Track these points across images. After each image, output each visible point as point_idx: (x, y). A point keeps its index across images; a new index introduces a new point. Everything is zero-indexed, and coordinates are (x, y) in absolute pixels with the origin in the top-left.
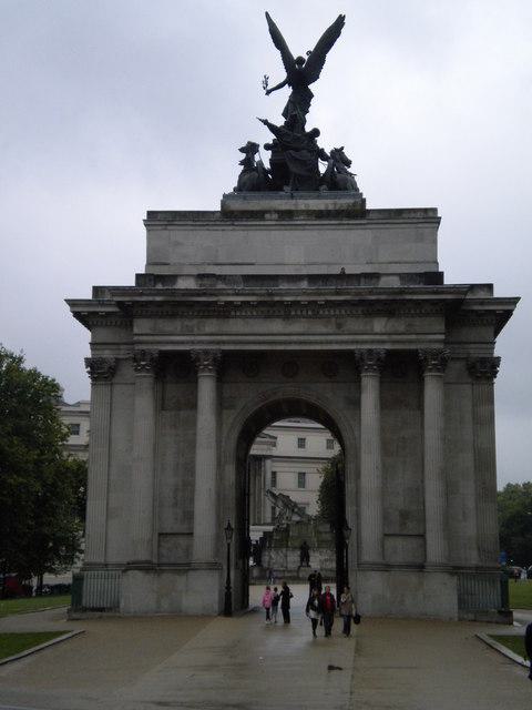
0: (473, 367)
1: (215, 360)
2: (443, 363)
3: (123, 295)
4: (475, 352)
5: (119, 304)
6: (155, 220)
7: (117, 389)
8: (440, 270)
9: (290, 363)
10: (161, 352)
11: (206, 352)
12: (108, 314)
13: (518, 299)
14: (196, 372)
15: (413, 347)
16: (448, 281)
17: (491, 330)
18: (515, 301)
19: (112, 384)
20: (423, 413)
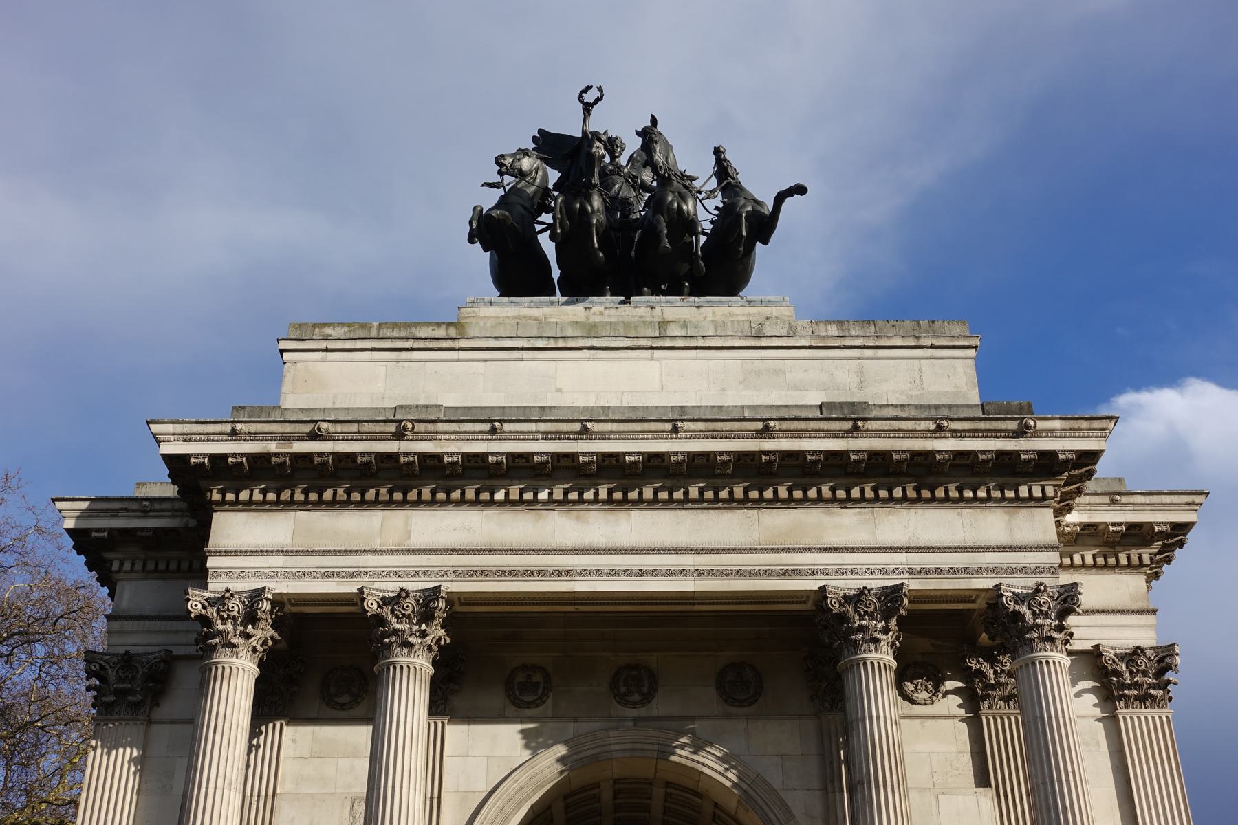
0: (1116, 673)
3: (187, 438)
5: (176, 464)
10: (279, 602)
11: (403, 593)
19: (150, 722)
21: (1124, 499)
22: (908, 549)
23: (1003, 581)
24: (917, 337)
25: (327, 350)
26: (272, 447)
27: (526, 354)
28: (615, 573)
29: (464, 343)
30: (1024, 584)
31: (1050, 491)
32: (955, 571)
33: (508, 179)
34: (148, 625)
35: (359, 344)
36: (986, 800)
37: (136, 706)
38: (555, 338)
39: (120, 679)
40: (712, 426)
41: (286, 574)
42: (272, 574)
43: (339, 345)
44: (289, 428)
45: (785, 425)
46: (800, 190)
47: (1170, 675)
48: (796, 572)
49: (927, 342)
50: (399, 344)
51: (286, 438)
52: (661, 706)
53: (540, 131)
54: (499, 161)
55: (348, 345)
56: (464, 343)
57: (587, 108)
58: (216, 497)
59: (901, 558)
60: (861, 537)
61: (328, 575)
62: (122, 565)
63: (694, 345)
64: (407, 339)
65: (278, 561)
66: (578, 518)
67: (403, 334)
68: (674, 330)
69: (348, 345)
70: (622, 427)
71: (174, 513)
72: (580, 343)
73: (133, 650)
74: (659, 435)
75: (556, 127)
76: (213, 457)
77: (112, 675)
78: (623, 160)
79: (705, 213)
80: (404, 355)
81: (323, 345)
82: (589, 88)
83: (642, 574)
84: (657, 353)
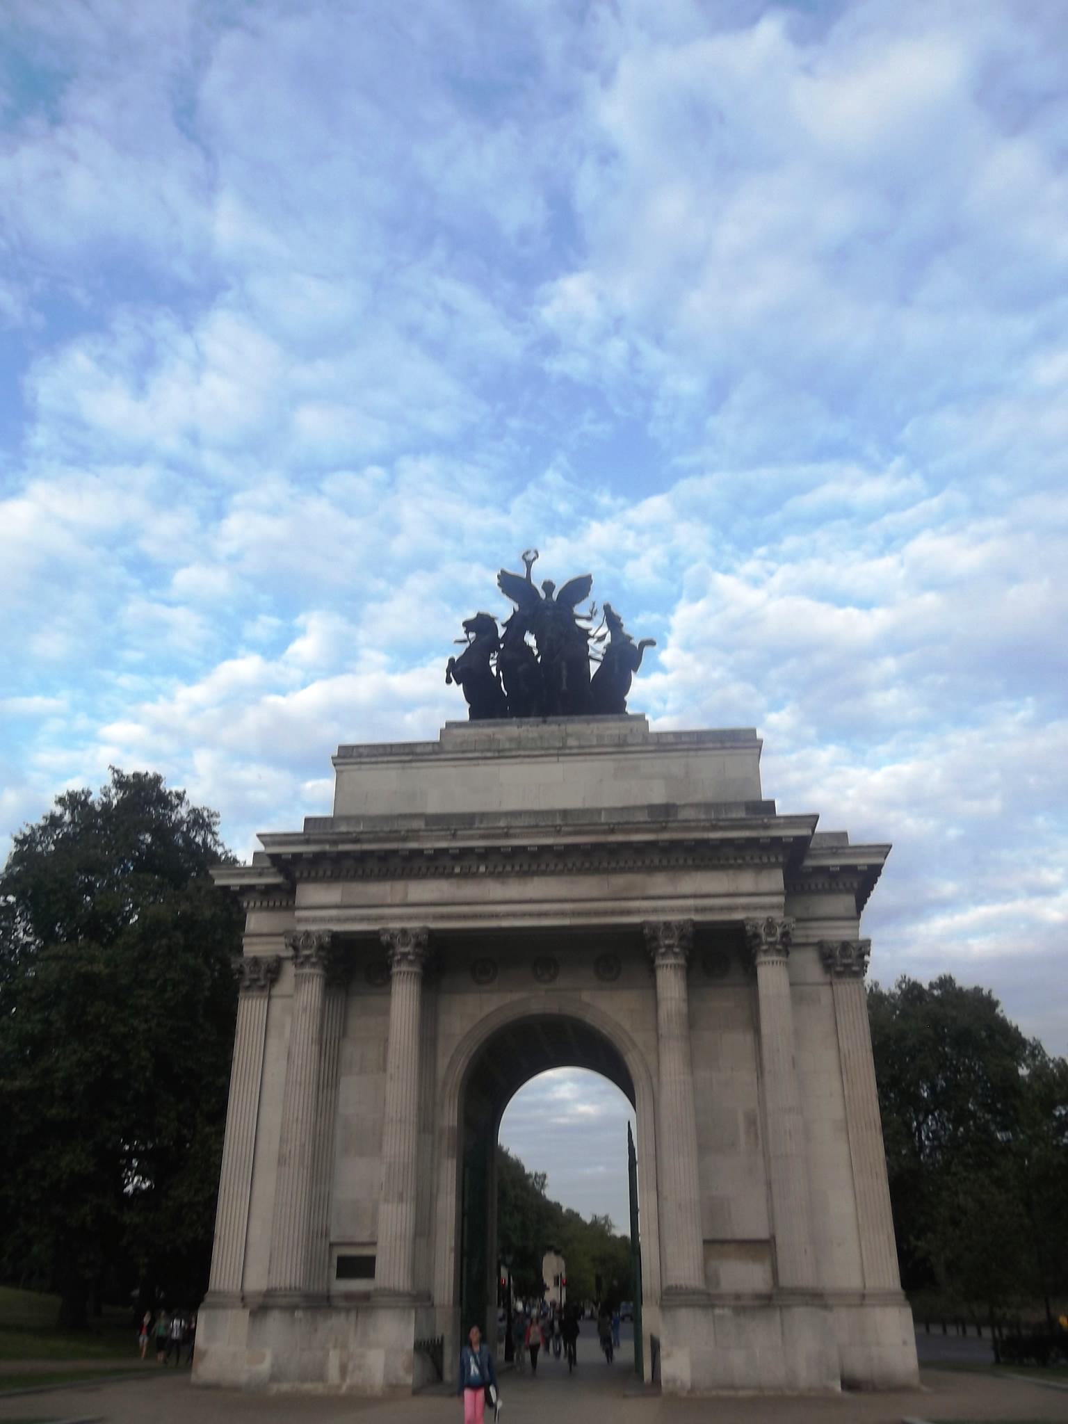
1: (418, 945)
2: (786, 945)
3: (281, 843)
4: (835, 933)
5: (275, 858)
6: (347, 757)
7: (277, 1004)
8: (765, 797)
10: (335, 936)
11: (404, 932)
14: (389, 968)
15: (739, 916)
17: (849, 901)
18: (884, 850)
19: (270, 998)
20: (757, 1031)
21: (840, 851)
22: (695, 896)
23: (752, 914)
26: (327, 848)
27: (480, 762)
28: (523, 915)
29: (443, 756)
30: (761, 916)
31: (781, 859)
32: (722, 909)
33: (472, 635)
34: (264, 939)
35: (380, 759)
36: (749, 1038)
37: (262, 988)
38: (499, 751)
39: (251, 972)
40: (578, 828)
41: (339, 920)
42: (330, 920)
44: (335, 837)
45: (620, 827)
47: (866, 958)
49: (728, 744)
51: (335, 843)
54: (466, 624)
55: (374, 759)
56: (443, 756)
57: (529, 564)
58: (298, 874)
59: (690, 902)
60: (669, 890)
61: (363, 919)
62: (248, 904)
63: (584, 751)
64: (408, 754)
65: (334, 913)
66: (503, 883)
67: (407, 750)
68: (572, 742)
70: (525, 830)
71: (274, 875)
72: (514, 753)
73: (259, 954)
74: (547, 834)
75: (510, 571)
77: (247, 969)
78: (555, 596)
79: (597, 649)
80: (407, 765)
81: (358, 760)
83: (541, 915)
84: (561, 759)
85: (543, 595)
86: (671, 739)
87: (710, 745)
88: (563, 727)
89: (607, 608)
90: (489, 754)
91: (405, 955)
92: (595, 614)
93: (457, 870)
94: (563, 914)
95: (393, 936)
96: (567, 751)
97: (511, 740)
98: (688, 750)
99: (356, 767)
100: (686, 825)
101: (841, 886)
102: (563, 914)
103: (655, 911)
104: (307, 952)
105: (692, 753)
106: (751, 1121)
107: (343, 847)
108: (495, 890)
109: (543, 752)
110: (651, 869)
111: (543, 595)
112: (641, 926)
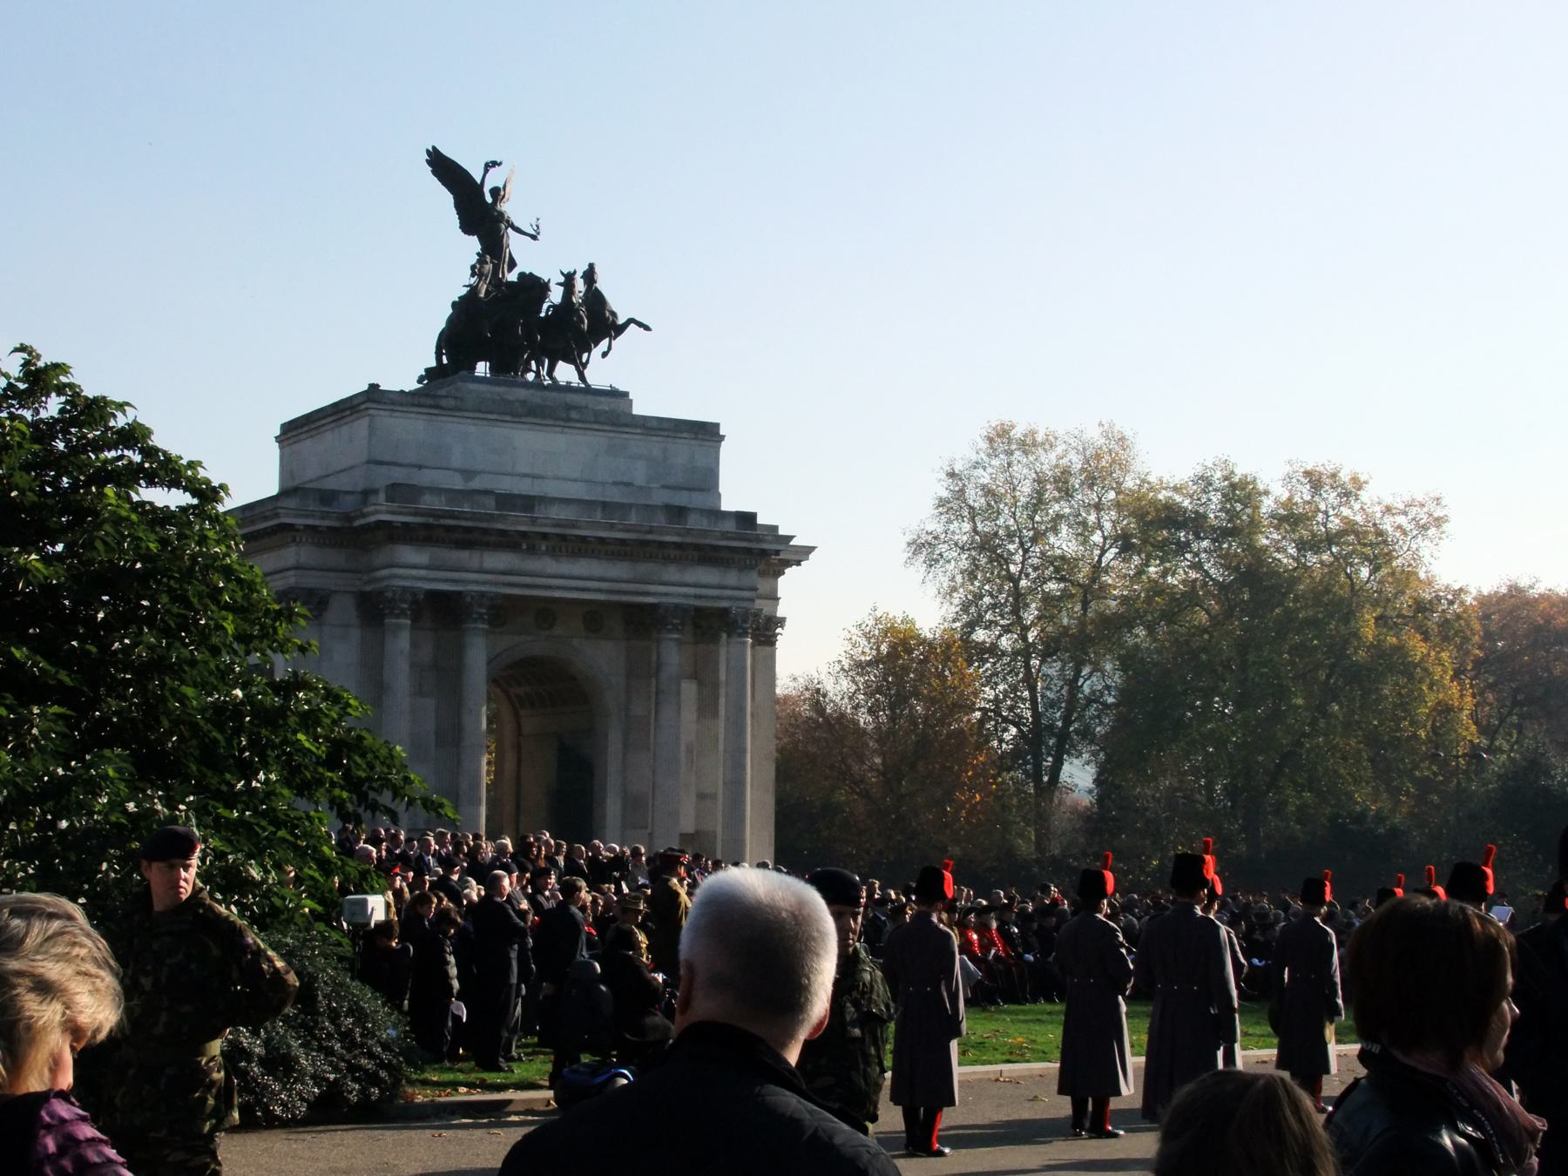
3: (393, 513)
9: (546, 612)
12: (330, 528)
13: (813, 548)
15: (724, 604)
16: (760, 521)
22: (695, 586)
24: (696, 434)
25: (393, 410)
26: (431, 520)
35: (411, 409)
43: (400, 408)
46: (647, 328)
48: (647, 594)
49: (700, 436)
50: (432, 411)
51: (439, 517)
52: (558, 630)
53: (434, 148)
56: (466, 414)
57: (486, 171)
59: (692, 591)
61: (446, 581)
65: (423, 573)
68: (574, 415)
69: (405, 409)
76: (403, 523)
80: (434, 418)
82: (495, 164)
84: (566, 430)
85: (489, 199)
86: (655, 424)
87: (685, 435)
88: (563, 395)
89: (591, 266)
90: (508, 418)
91: (481, 615)
92: (538, 233)
93: (524, 547)
94: (599, 591)
95: (473, 598)
96: (572, 425)
97: (524, 403)
98: (668, 436)
99: (387, 413)
100: (705, 533)
101: (771, 572)
102: (599, 591)
103: (666, 595)
104: (405, 606)
105: (669, 440)
106: (690, 750)
107: (442, 522)
108: (549, 565)
109: (551, 422)
110: (668, 560)
111: (489, 199)
112: (654, 606)
